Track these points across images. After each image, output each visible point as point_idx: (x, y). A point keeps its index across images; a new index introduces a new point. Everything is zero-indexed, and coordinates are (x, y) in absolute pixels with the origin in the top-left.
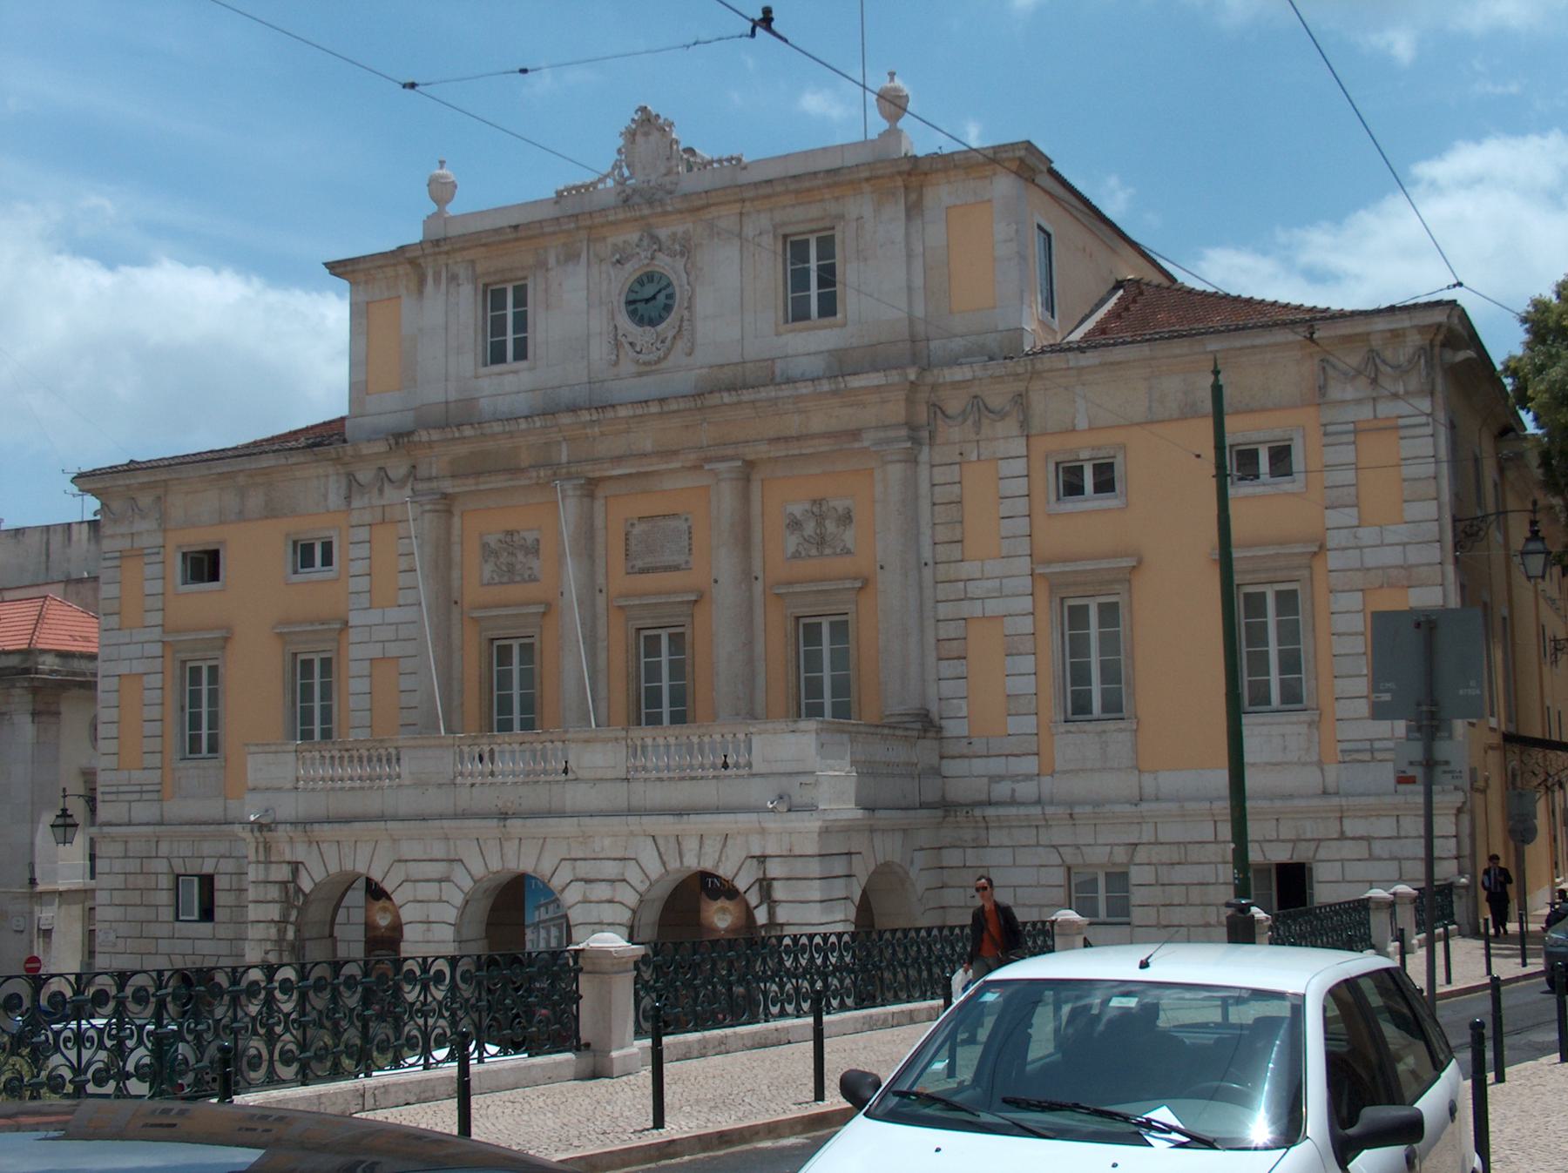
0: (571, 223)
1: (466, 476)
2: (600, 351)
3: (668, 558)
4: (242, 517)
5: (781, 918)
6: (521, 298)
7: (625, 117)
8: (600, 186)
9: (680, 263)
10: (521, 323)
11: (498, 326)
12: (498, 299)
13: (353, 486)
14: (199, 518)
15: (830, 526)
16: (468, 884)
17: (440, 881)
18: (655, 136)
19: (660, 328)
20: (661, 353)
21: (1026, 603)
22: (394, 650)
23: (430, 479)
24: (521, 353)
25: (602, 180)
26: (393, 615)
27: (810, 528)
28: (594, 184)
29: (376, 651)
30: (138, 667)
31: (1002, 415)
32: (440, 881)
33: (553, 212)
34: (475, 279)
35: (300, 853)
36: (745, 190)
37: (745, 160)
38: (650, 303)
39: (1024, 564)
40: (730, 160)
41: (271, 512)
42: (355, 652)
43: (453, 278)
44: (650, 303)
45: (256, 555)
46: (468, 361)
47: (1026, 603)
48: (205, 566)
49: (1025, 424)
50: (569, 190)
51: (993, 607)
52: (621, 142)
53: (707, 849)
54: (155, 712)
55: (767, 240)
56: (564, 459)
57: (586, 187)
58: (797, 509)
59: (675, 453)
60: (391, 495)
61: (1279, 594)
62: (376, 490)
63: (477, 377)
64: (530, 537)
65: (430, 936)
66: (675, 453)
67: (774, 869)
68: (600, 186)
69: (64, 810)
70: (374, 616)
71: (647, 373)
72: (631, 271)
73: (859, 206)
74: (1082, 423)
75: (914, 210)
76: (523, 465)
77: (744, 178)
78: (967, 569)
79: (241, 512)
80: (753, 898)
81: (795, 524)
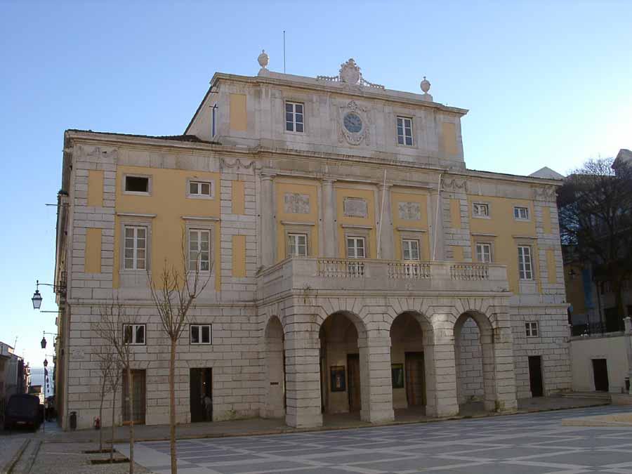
0: (318, 88)
1: (287, 170)
2: (334, 137)
3: (358, 213)
4: (162, 166)
5: (500, 325)
6: (299, 109)
7: (345, 60)
8: (333, 80)
9: (365, 114)
10: (299, 119)
11: (289, 117)
12: (289, 108)
13: (222, 165)
14: (139, 163)
15: (413, 211)
16: (395, 316)
17: (383, 314)
18: (354, 70)
19: (359, 133)
20: (357, 143)
21: (469, 243)
22: (243, 232)
23: (270, 167)
24: (300, 129)
25: (334, 78)
26: (242, 218)
27: (407, 210)
28: (331, 79)
29: (236, 232)
30: (98, 225)
31: (460, 187)
32: (383, 314)
33: (317, 83)
34: (282, 98)
35: (320, 301)
36: (380, 97)
37: (386, 88)
38: (352, 123)
39: (468, 232)
40: (379, 86)
41: (179, 167)
42: (223, 231)
43: (273, 95)
44: (352, 123)
45: (168, 182)
46: (281, 127)
47: (469, 243)
48: (136, 184)
49: (466, 190)
50: (322, 77)
51: (461, 243)
52: (341, 68)
53: (477, 303)
54: (111, 247)
55: (392, 115)
56: (327, 171)
57: (328, 78)
58: (402, 204)
59: (370, 177)
60: (242, 170)
61: (525, 249)
62: (235, 168)
63: (284, 133)
64: (304, 198)
65: (380, 335)
66: (370, 177)
67: (498, 310)
68: (333, 80)
69: (37, 291)
70: (234, 218)
71: (353, 148)
72: (347, 111)
73: (420, 113)
74: (480, 194)
75: (435, 118)
76: (310, 170)
77: (384, 93)
78: (453, 230)
79: (161, 164)
80: (491, 320)
81: (401, 209)
